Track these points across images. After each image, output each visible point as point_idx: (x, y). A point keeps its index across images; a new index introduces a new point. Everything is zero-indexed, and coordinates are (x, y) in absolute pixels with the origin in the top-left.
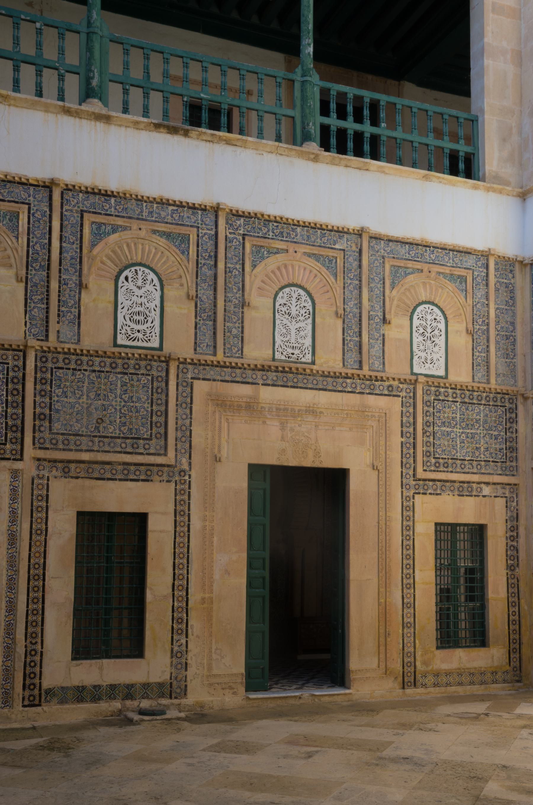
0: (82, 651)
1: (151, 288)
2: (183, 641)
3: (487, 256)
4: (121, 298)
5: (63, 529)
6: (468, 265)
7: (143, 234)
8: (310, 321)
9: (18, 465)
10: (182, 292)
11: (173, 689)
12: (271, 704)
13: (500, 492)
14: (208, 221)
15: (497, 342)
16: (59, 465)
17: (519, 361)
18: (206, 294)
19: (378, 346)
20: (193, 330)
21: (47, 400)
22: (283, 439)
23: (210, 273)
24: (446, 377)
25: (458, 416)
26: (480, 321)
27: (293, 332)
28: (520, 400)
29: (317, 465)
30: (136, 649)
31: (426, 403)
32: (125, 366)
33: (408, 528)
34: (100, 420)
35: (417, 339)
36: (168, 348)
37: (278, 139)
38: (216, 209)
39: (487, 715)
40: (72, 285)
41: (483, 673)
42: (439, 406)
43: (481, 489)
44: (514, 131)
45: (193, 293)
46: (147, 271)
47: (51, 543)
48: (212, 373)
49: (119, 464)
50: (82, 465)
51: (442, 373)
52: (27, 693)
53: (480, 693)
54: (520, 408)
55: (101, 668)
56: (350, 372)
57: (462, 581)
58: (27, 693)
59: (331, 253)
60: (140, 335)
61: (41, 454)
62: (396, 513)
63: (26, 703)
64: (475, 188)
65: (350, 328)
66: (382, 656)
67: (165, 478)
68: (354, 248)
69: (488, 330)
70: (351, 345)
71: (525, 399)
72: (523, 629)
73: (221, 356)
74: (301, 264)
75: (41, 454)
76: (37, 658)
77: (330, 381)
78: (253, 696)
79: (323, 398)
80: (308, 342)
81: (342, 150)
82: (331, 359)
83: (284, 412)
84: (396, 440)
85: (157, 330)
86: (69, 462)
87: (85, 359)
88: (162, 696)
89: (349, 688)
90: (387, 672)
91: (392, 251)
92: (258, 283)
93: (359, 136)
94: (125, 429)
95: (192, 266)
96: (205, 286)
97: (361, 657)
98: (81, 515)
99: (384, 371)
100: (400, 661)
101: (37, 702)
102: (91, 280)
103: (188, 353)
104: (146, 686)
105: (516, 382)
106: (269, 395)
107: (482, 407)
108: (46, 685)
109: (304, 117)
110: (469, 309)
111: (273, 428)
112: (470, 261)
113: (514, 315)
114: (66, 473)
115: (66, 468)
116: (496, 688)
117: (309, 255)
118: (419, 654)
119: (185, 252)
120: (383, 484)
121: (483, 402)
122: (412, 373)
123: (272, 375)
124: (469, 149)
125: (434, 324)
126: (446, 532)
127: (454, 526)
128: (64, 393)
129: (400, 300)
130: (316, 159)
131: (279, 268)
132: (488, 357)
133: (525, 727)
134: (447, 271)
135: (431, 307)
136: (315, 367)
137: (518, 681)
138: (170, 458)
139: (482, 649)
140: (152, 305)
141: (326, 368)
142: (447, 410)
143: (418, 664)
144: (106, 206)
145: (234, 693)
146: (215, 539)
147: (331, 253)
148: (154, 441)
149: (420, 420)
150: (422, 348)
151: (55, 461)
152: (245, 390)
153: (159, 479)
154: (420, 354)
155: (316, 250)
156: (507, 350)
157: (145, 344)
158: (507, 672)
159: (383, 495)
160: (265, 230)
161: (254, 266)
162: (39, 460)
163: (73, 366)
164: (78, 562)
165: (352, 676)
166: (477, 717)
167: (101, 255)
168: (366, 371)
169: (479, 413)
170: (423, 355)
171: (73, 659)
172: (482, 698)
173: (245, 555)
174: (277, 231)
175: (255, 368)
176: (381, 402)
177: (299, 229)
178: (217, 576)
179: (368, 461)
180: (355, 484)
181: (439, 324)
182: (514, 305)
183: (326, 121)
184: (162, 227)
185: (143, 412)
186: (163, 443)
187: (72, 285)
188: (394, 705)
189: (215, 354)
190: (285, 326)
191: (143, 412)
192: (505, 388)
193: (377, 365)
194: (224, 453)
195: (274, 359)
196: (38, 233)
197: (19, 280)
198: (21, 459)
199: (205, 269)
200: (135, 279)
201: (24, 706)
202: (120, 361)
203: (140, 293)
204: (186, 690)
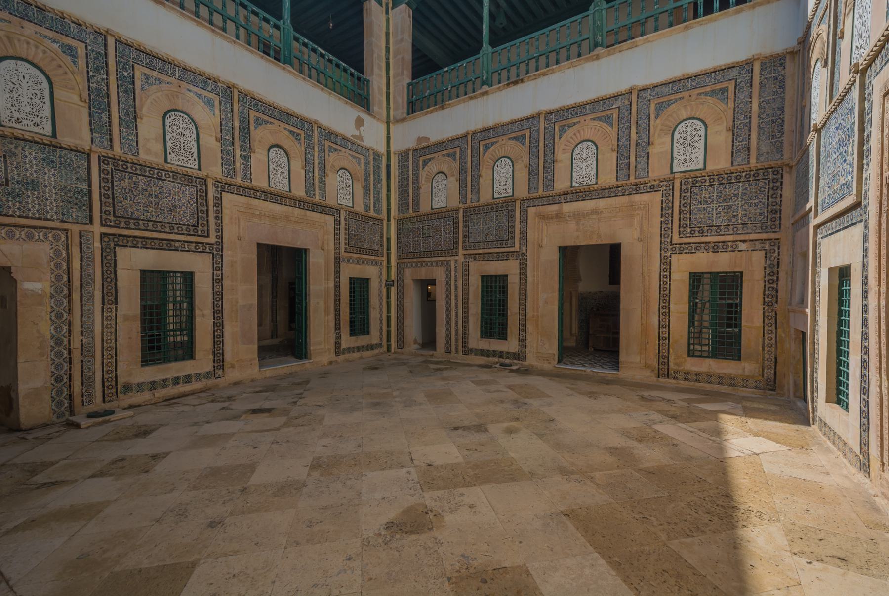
3: (752, 62)
5: (475, 283)
6: (731, 77)
7: (504, 142)
9: (457, 258)
11: (519, 356)
12: (569, 372)
13: (758, 245)
14: (535, 122)
19: (643, 162)
22: (577, 230)
24: (705, 168)
25: (715, 194)
27: (584, 167)
29: (599, 242)
33: (665, 277)
34: (487, 234)
38: (539, 115)
42: (696, 191)
43: (737, 246)
48: (537, 202)
51: (701, 166)
56: (620, 183)
59: (609, 112)
65: (622, 155)
68: (627, 102)
69: (750, 123)
71: (791, 167)
73: (544, 192)
74: (589, 127)
75: (465, 252)
79: (602, 203)
80: (593, 172)
82: (609, 178)
83: (578, 216)
88: (515, 359)
91: (657, 94)
95: (527, 150)
97: (630, 355)
98: (483, 277)
99: (648, 176)
102: (483, 172)
104: (508, 353)
105: (782, 155)
106: (567, 208)
107: (741, 184)
110: (731, 112)
111: (572, 225)
112: (734, 73)
113: (783, 99)
115: (475, 257)
117: (594, 119)
118: (672, 358)
121: (742, 180)
125: (694, 133)
131: (575, 134)
134: (708, 89)
135: (691, 121)
138: (517, 248)
142: (704, 192)
143: (671, 364)
144: (488, 135)
150: (682, 152)
152: (555, 208)
154: (679, 158)
155: (598, 115)
156: (773, 131)
160: (566, 115)
161: (560, 138)
167: (487, 158)
168: (632, 179)
176: (645, 197)
179: (636, 235)
181: (699, 133)
182: (783, 92)
184: (512, 135)
190: (579, 166)
192: (766, 165)
194: (545, 242)
195: (572, 187)
203: (504, 171)
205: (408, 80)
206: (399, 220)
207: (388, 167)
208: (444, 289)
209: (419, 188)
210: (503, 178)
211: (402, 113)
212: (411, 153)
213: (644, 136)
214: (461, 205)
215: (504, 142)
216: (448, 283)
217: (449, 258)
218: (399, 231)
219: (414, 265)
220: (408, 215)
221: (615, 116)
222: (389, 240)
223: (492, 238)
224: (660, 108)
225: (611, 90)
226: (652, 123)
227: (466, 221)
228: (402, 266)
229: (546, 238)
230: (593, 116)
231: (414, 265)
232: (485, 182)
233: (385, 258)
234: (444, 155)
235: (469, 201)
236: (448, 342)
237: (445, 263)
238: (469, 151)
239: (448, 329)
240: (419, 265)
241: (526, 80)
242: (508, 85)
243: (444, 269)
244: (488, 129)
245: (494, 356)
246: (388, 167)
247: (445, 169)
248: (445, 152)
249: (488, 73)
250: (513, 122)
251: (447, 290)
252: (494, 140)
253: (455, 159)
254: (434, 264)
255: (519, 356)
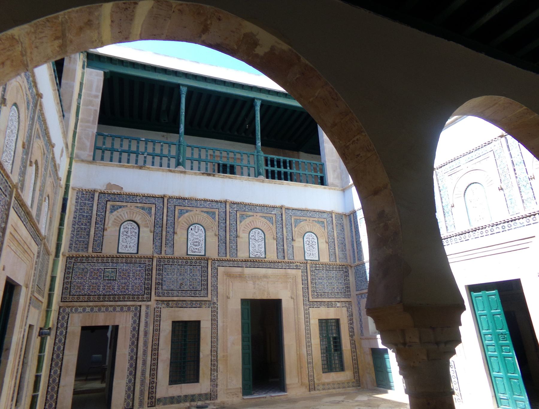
0: (173, 381)
1: (201, 232)
2: (216, 374)
4: (189, 237)
5: (166, 328)
6: (324, 217)
7: (198, 212)
8: (263, 241)
9: (149, 303)
10: (213, 233)
11: (211, 396)
13: (344, 304)
14: (222, 206)
15: (338, 246)
16: (165, 302)
17: (347, 252)
18: (222, 233)
20: (217, 248)
21: (161, 277)
22: (254, 288)
23: (224, 225)
26: (331, 238)
27: (257, 246)
28: (349, 267)
30: (196, 379)
31: (311, 271)
32: (191, 262)
34: (182, 284)
35: (306, 246)
36: (207, 255)
37: (249, 175)
38: (226, 202)
39: (343, 401)
40: (171, 233)
41: (343, 383)
42: (317, 272)
44: (338, 168)
45: (217, 233)
46: (199, 226)
47: (161, 334)
48: (225, 264)
49: (189, 301)
50: (174, 302)
51: (317, 259)
52: (150, 401)
53: (343, 392)
54: (350, 271)
55: (181, 388)
56: (280, 260)
57: (332, 343)
58: (150, 401)
59: (271, 215)
60: (197, 250)
61: (158, 298)
62: (302, 316)
63: (149, 405)
64: (325, 188)
65: (279, 243)
66: (300, 377)
67: (207, 306)
70: (280, 250)
71: (351, 267)
72: (359, 362)
73: (228, 256)
74: (259, 221)
75: (158, 298)
76: (154, 385)
77: (272, 264)
78: (246, 397)
79: (270, 271)
80: (263, 250)
81: (273, 178)
82: (272, 256)
83: (255, 278)
84: (300, 286)
85: (203, 248)
86: (169, 301)
87: (175, 260)
88: (207, 399)
89: (286, 392)
90: (302, 384)
91: (294, 214)
92: (242, 228)
93: (279, 173)
94: (191, 287)
95: (217, 223)
96: (222, 230)
100: (307, 379)
101: (153, 405)
102: (178, 230)
103: (215, 256)
104: (200, 395)
106: (248, 271)
108: (158, 396)
109: (258, 167)
111: (250, 284)
112: (325, 215)
114: (168, 305)
115: (168, 303)
116: (350, 390)
117: (262, 217)
119: (214, 218)
120: (296, 305)
122: (305, 260)
123: (249, 263)
124: (322, 175)
126: (324, 324)
127: (327, 320)
128: (167, 274)
129: (298, 231)
130: (263, 182)
132: (335, 251)
133: (358, 405)
134: (316, 219)
136: (266, 259)
137: (359, 386)
138: (209, 298)
139: (342, 372)
140: (201, 239)
141: (270, 260)
143: (315, 380)
145: (238, 397)
146: (228, 330)
147: (271, 215)
148: (202, 292)
149: (309, 278)
151: (163, 301)
152: (239, 270)
153: (204, 306)
157: (199, 254)
158: (354, 382)
159: (296, 309)
160: (245, 208)
161: (241, 222)
162: (157, 301)
163: (171, 263)
164: (173, 342)
165: (288, 387)
166: (338, 403)
168: (286, 260)
169: (333, 274)
170: (309, 252)
171: (169, 384)
172: (342, 394)
173: (240, 336)
174: (249, 209)
175: (242, 261)
176: (293, 272)
177: (258, 207)
178: (229, 345)
179: (289, 295)
180: (284, 305)
182: (344, 231)
183: (267, 168)
184: (205, 210)
185: (198, 280)
186: (206, 292)
187: (171, 233)
188: (305, 399)
189: (226, 256)
190: (254, 244)
191: (198, 280)
192: (343, 263)
193: (291, 257)
194: (231, 295)
195: (250, 257)
196: (158, 214)
197: (151, 232)
198: (150, 301)
199: (222, 224)
200: (195, 229)
201: (148, 407)
202: (189, 261)
203: (197, 235)
204: (217, 396)
205: (94, 128)
206: (69, 258)
207: (65, 200)
208: (129, 336)
209: (104, 229)
210: (196, 239)
211: (89, 156)
212: (96, 195)
213: (290, 235)
214: (156, 255)
215: (198, 212)
216: (136, 330)
217: (140, 303)
218: (68, 270)
219: (88, 309)
220: (85, 254)
221: (274, 219)
222: (53, 279)
223: (186, 288)
224: (297, 222)
225: (272, 204)
226: (293, 229)
227: (159, 270)
228: (68, 310)
229: (234, 292)
230: (261, 214)
231: (88, 309)
232: (179, 238)
233: (45, 301)
234: (137, 207)
235: (163, 252)
236: (128, 397)
237: (133, 308)
238: (165, 211)
239: (130, 381)
240: (96, 309)
241: (216, 176)
242: (203, 174)
243: (131, 314)
244: (184, 199)
245: (185, 401)
246: (65, 200)
247: (137, 219)
248: (140, 205)
249: (183, 157)
250: (205, 201)
251: (133, 336)
252: (189, 208)
253: (150, 213)
254: (118, 309)
255: (211, 396)
